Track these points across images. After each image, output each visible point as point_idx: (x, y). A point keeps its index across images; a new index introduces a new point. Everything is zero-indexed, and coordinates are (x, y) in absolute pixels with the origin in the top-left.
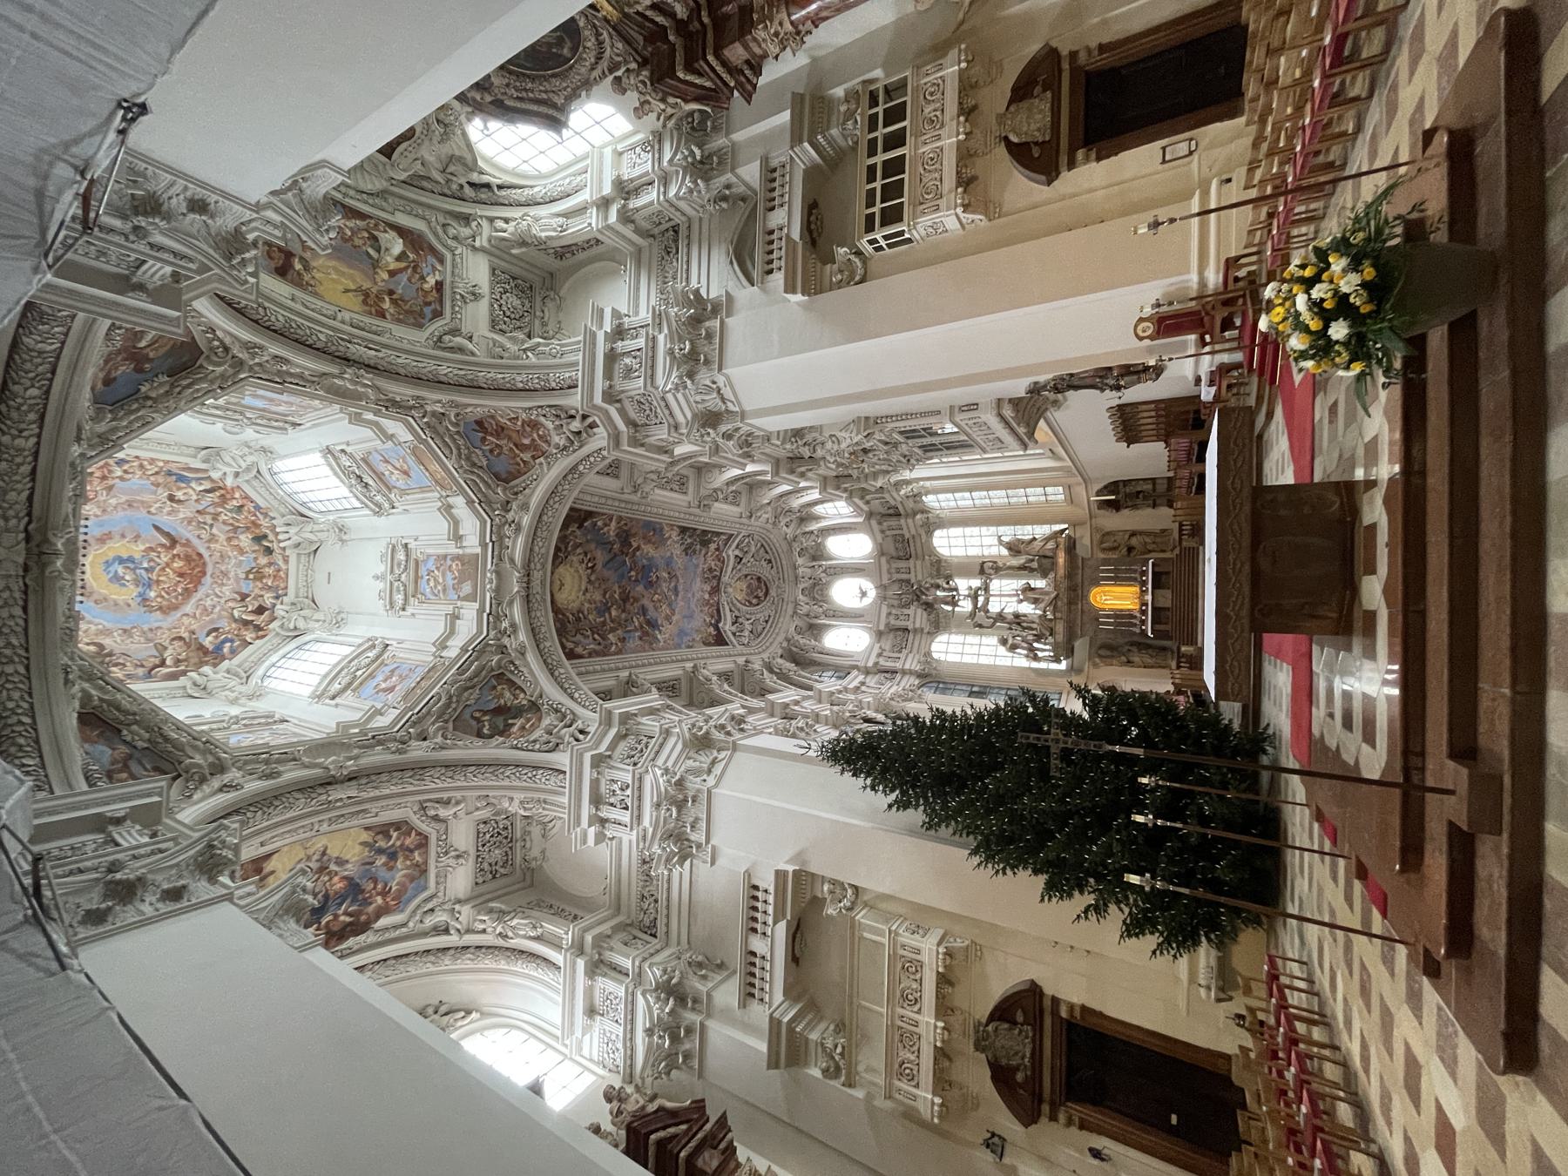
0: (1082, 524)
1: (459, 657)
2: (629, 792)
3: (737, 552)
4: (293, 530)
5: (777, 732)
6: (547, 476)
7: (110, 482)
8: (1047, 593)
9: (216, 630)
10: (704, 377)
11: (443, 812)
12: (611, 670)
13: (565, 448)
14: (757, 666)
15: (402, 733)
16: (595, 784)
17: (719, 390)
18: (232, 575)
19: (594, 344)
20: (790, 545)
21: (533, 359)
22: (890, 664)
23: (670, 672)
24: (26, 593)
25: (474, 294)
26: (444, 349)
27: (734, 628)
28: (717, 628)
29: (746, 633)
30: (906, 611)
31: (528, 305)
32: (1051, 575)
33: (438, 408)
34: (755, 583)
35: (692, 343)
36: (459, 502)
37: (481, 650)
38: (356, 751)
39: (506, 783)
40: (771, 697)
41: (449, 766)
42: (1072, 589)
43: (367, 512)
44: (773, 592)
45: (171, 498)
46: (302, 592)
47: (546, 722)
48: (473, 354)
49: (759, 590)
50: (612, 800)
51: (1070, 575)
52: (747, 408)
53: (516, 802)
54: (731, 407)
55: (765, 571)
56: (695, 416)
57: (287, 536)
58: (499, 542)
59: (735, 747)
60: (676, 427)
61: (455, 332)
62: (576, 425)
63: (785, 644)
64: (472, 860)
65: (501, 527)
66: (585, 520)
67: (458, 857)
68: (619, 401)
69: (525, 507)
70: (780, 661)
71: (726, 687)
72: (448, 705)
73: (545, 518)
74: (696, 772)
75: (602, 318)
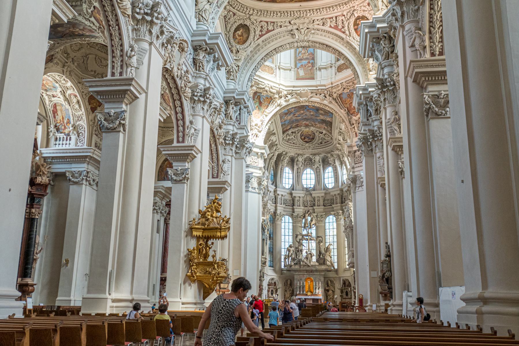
0: (337, 274)
8: (310, 262)
20: (329, 153)
22: (279, 200)
29: (288, 137)
30: (301, 205)
32: (317, 264)
34: (311, 137)
42: (312, 271)
49: (308, 139)
51: (317, 271)
52: (357, 193)
54: (357, 188)
55: (316, 141)
56: (356, 176)
58: (317, 93)
63: (284, 153)
69: (331, 102)
72: (261, 88)
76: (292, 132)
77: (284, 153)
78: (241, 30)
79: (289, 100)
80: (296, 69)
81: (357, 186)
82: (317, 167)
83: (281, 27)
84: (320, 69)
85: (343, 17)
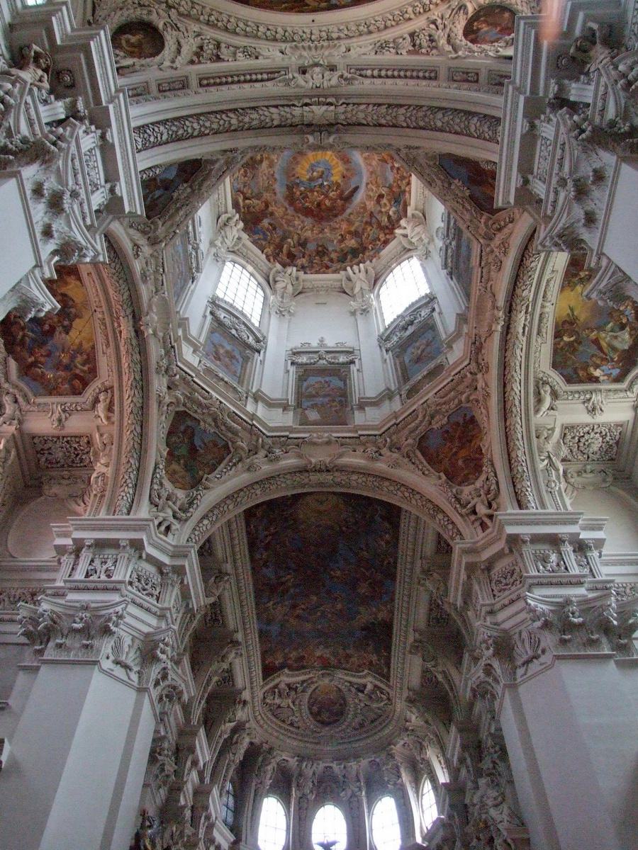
1: (246, 413)
2: (103, 577)
3: (369, 687)
4: (362, 275)
5: (157, 740)
6: (430, 485)
7: (389, 161)
9: (275, 229)
10: (549, 640)
11: (101, 407)
12: (234, 554)
13: (458, 500)
14: (241, 714)
15: (175, 369)
16: (114, 544)
17: (536, 657)
18: (320, 236)
19: (565, 523)
21: (542, 465)
23: (232, 618)
24: (291, 126)
25: (594, 409)
26: (537, 386)
27: (282, 686)
28: (282, 667)
29: (277, 701)
31: (595, 457)
33: (480, 384)
35: (580, 625)
36: (396, 405)
37: (251, 430)
38: (161, 334)
39: (124, 460)
40: (202, 732)
41: (143, 410)
43: (382, 330)
44: (326, 731)
45: (381, 196)
46: (308, 285)
47: (181, 494)
48: (537, 411)
49: (328, 712)
50: (97, 563)
52: (521, 689)
53: (104, 470)
54: (520, 671)
55: (351, 718)
56: (505, 631)
57: (358, 273)
58: (359, 441)
59: (141, 690)
60: (491, 613)
61: (555, 395)
62: (482, 510)
63: (266, 747)
64: (56, 432)
65: (375, 443)
66: (391, 523)
67: (60, 420)
68: (511, 551)
69: (396, 465)
70: (247, 740)
71: (215, 679)
72: (200, 405)
73: (387, 483)
74: (117, 648)
75: (593, 529)
76: (288, 685)
77: (266, 747)
78: (138, 37)
79: (277, 459)
80: (300, 410)
81: (519, 663)
82: (353, 795)
83: (257, 58)
84: (362, 407)
85: (433, 26)
